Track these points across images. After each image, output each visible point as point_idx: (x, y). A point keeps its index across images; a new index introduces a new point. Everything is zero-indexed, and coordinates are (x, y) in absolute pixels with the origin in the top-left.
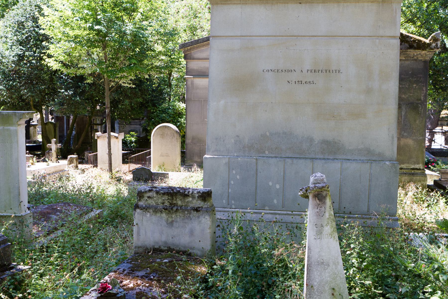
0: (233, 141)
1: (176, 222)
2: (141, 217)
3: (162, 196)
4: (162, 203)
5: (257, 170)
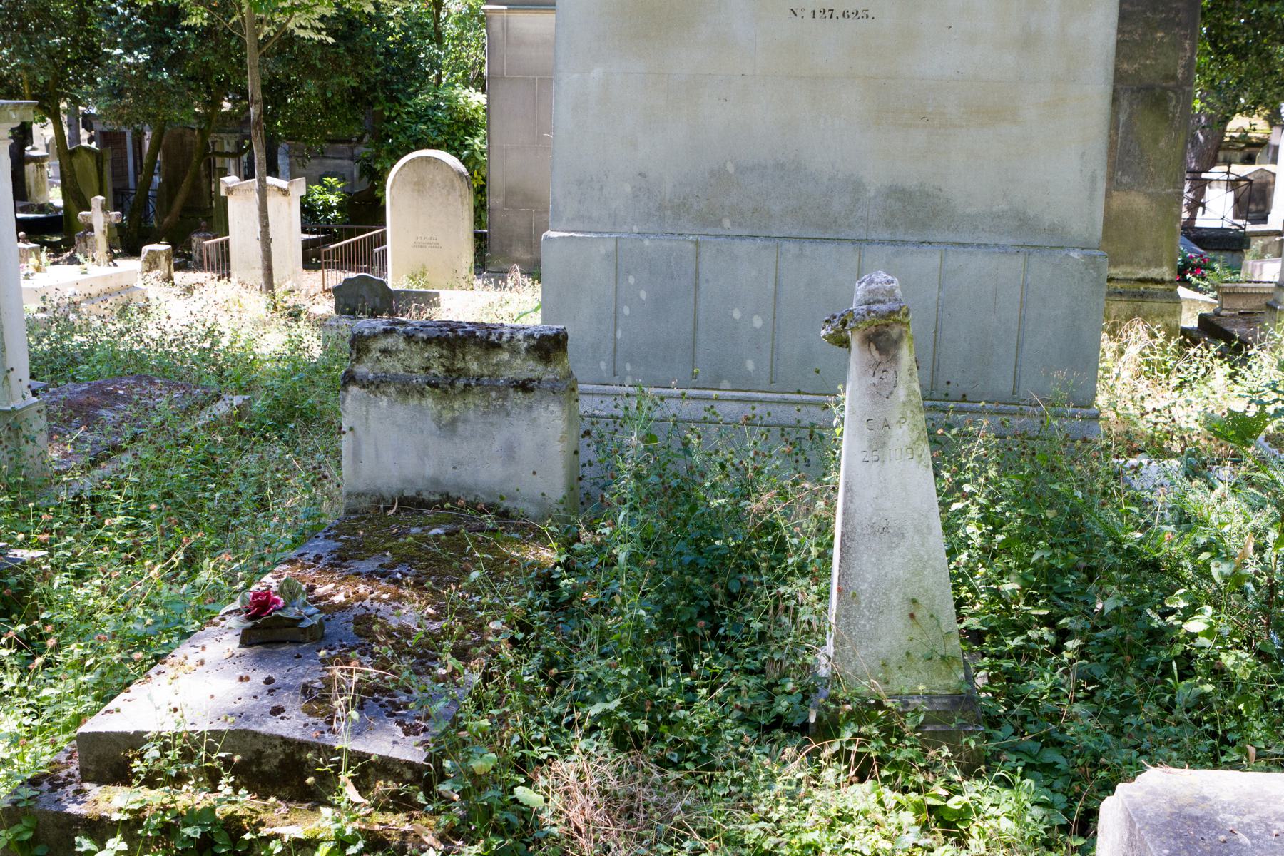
0: (628, 188)
1: (466, 421)
2: (364, 408)
3: (421, 349)
4: (423, 368)
5: (697, 273)
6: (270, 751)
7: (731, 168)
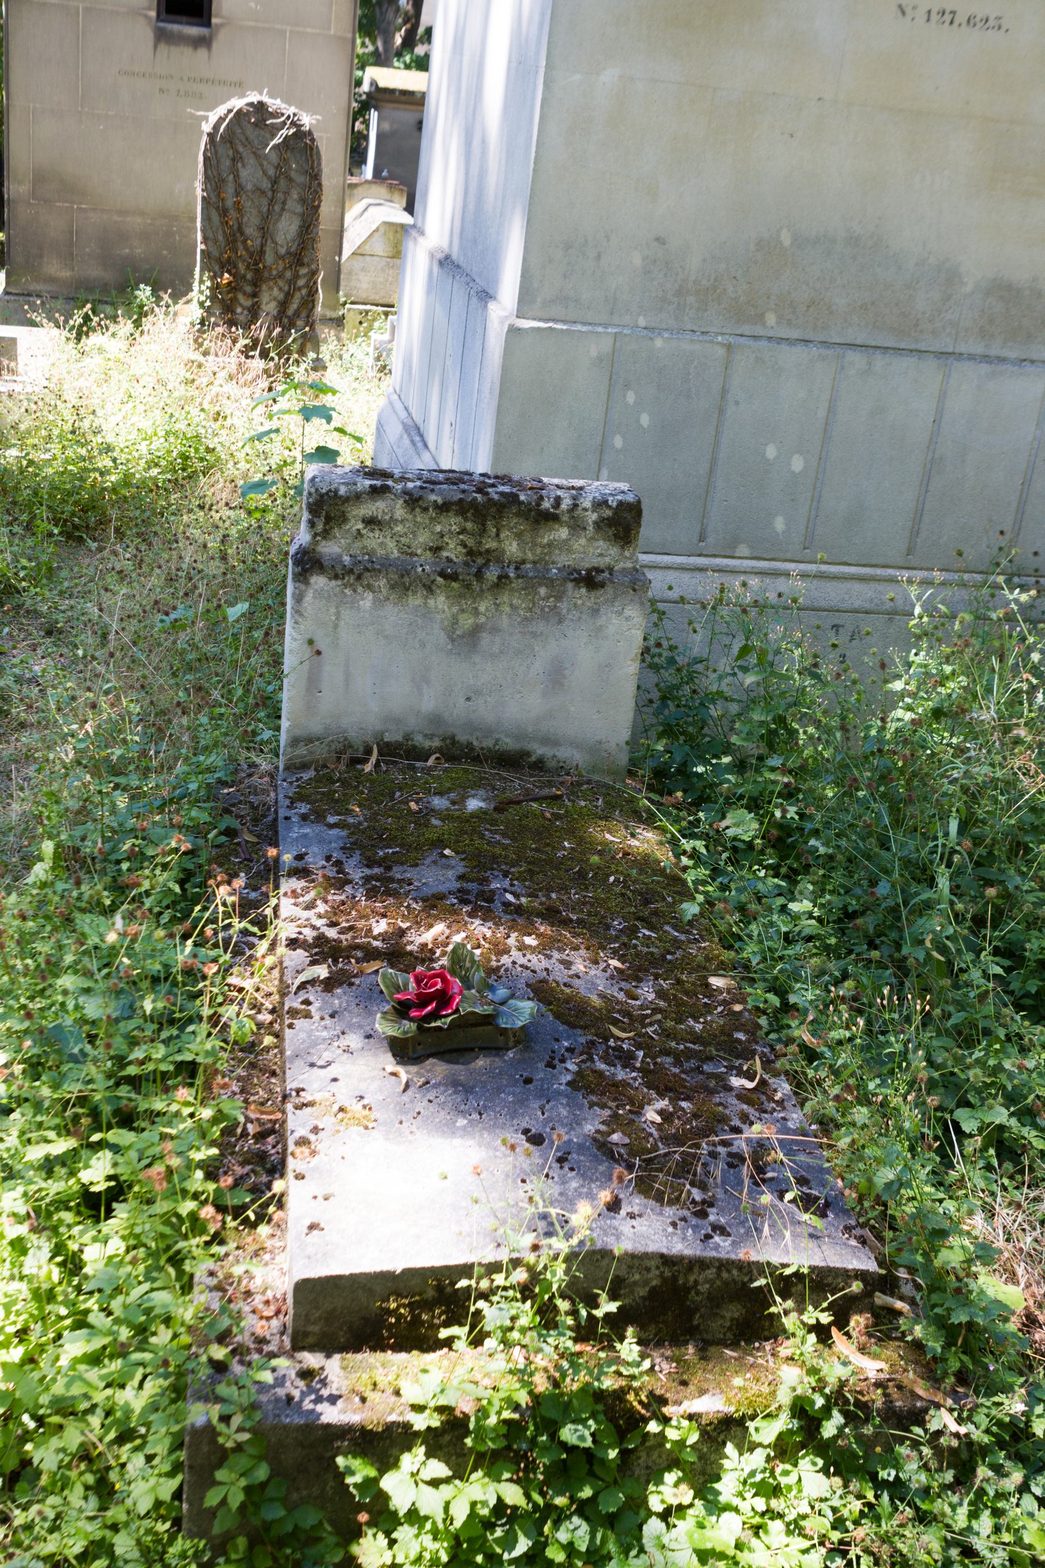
0: (637, 261)
1: (495, 630)
2: (333, 610)
3: (431, 519)
4: (431, 549)
5: (724, 391)
6: (637, 1277)
7: (786, 239)
